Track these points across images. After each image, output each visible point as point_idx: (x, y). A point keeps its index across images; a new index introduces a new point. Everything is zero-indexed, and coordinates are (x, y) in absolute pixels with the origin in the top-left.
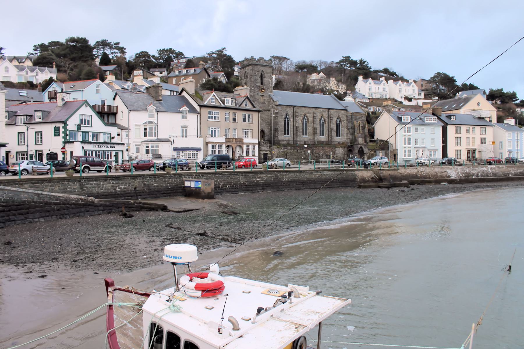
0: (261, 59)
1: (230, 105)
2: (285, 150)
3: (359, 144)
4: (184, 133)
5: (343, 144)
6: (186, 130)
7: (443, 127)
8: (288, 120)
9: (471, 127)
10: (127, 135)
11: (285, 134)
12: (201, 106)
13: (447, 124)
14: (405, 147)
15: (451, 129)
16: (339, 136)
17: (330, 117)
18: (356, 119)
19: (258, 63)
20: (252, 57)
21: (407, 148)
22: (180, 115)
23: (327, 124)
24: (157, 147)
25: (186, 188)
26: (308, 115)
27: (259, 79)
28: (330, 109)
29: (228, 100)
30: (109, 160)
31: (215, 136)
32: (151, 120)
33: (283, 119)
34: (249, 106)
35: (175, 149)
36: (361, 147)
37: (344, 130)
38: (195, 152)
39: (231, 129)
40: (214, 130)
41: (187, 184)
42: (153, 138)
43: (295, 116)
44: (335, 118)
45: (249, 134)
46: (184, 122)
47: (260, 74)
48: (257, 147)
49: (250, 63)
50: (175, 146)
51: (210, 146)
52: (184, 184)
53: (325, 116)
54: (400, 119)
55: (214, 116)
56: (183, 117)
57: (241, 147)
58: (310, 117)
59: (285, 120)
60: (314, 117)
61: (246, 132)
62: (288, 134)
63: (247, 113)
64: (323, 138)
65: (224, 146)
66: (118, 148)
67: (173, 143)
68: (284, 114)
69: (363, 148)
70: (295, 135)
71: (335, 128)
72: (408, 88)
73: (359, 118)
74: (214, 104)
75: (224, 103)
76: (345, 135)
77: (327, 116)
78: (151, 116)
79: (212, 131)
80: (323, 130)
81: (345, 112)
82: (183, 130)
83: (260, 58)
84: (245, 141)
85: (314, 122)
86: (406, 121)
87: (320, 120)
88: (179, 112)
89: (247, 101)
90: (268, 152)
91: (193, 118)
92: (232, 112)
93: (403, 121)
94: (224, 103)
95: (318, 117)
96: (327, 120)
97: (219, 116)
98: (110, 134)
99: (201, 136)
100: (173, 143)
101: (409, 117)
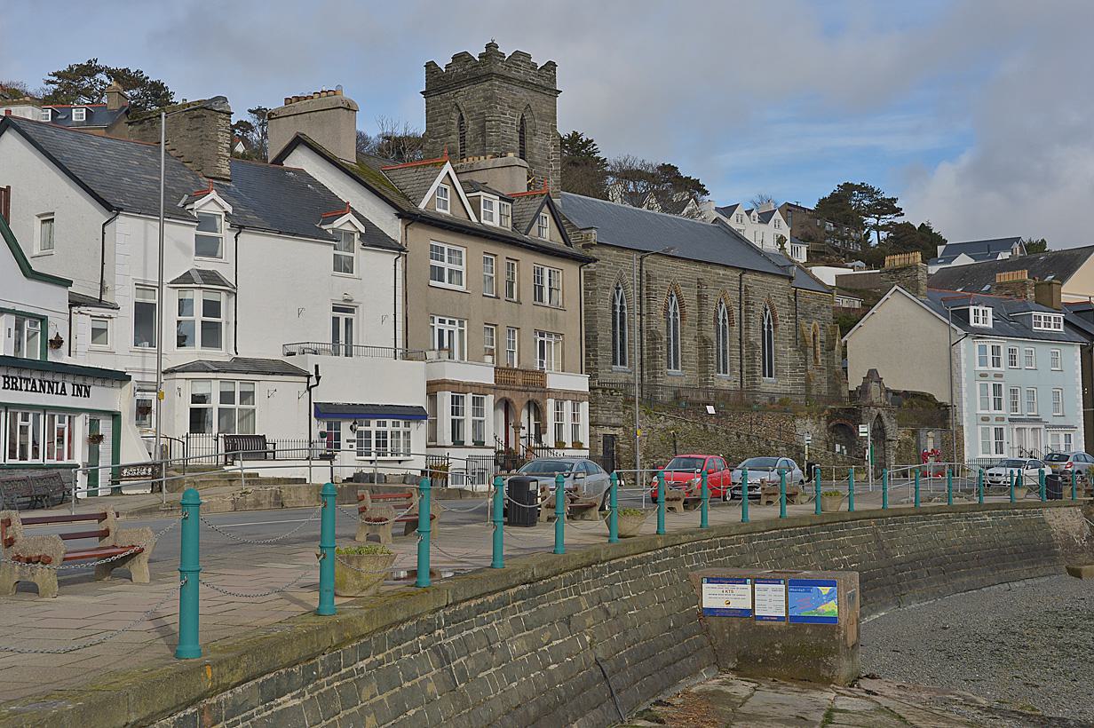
1: (496, 223)
2: (670, 423)
3: (872, 404)
4: (342, 336)
5: (782, 403)
6: (348, 322)
7: (1082, 348)
8: (622, 308)
10: (98, 333)
11: (615, 362)
12: (410, 218)
14: (985, 419)
16: (770, 376)
17: (745, 302)
18: (805, 316)
19: (513, 73)
20: (491, 47)
21: (993, 420)
22: (323, 253)
23: (736, 328)
24: (247, 396)
25: (714, 622)
26: (683, 290)
27: (516, 137)
28: (745, 270)
29: (489, 204)
30: (66, 461)
31: (462, 358)
32: (208, 264)
33: (609, 302)
34: (548, 233)
35: (323, 411)
36: (879, 416)
37: (785, 353)
38: (402, 428)
39: (503, 329)
40: (446, 328)
41: (714, 596)
42: (222, 355)
43: (646, 294)
44: (759, 308)
45: (553, 352)
46: (342, 287)
47: (517, 120)
48: (584, 407)
49: (483, 71)
50: (322, 395)
51: (445, 399)
52: (699, 597)
54: (961, 318)
55: (446, 265)
56: (343, 266)
57: (537, 409)
58: (690, 297)
59: (614, 307)
61: (542, 343)
62: (623, 363)
63: (547, 264)
64: (725, 381)
65: (489, 401)
66: (102, 397)
67: (313, 381)
68: (613, 284)
69: (885, 419)
70: (649, 364)
71: (760, 343)
72: (763, 226)
73: (816, 310)
74: (448, 212)
75: (478, 217)
76: (788, 371)
77: (734, 296)
78: (207, 247)
79: (441, 332)
80: (725, 351)
81: (786, 282)
82: (336, 321)
84: (555, 381)
86: (980, 324)
87: (717, 313)
88: (322, 236)
89: (545, 213)
90: (619, 431)
91: (376, 268)
92: (504, 252)
93: (972, 323)
94: (478, 217)
95: (712, 300)
96: (736, 313)
97: (463, 268)
98: (43, 319)
99: (407, 356)
100: (313, 381)
101: (990, 310)
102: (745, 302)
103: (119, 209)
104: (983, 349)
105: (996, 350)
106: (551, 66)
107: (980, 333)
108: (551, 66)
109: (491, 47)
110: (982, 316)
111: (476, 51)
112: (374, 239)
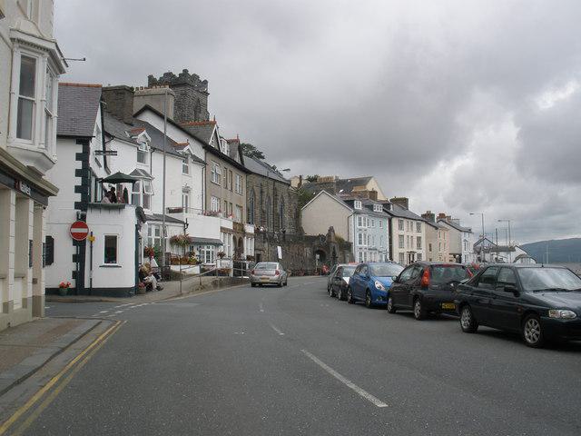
0: (195, 77)
6: (187, 197)
9: (410, 221)
13: (392, 215)
15: (395, 222)
17: (275, 195)
20: (185, 71)
22: (179, 164)
53: (271, 192)
54: (350, 203)
56: (186, 170)
60: (262, 192)
83: (194, 75)
85: (261, 204)
102: (275, 195)
103: (113, 137)
104: (360, 219)
105: (365, 219)
106: (206, 82)
107: (357, 213)
108: (206, 82)
109: (185, 71)
110: (358, 205)
111: (177, 73)
112: (197, 160)
